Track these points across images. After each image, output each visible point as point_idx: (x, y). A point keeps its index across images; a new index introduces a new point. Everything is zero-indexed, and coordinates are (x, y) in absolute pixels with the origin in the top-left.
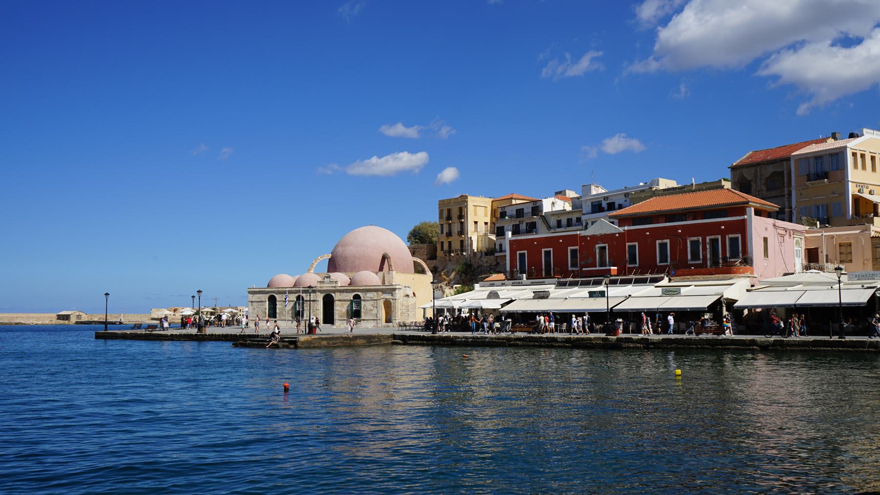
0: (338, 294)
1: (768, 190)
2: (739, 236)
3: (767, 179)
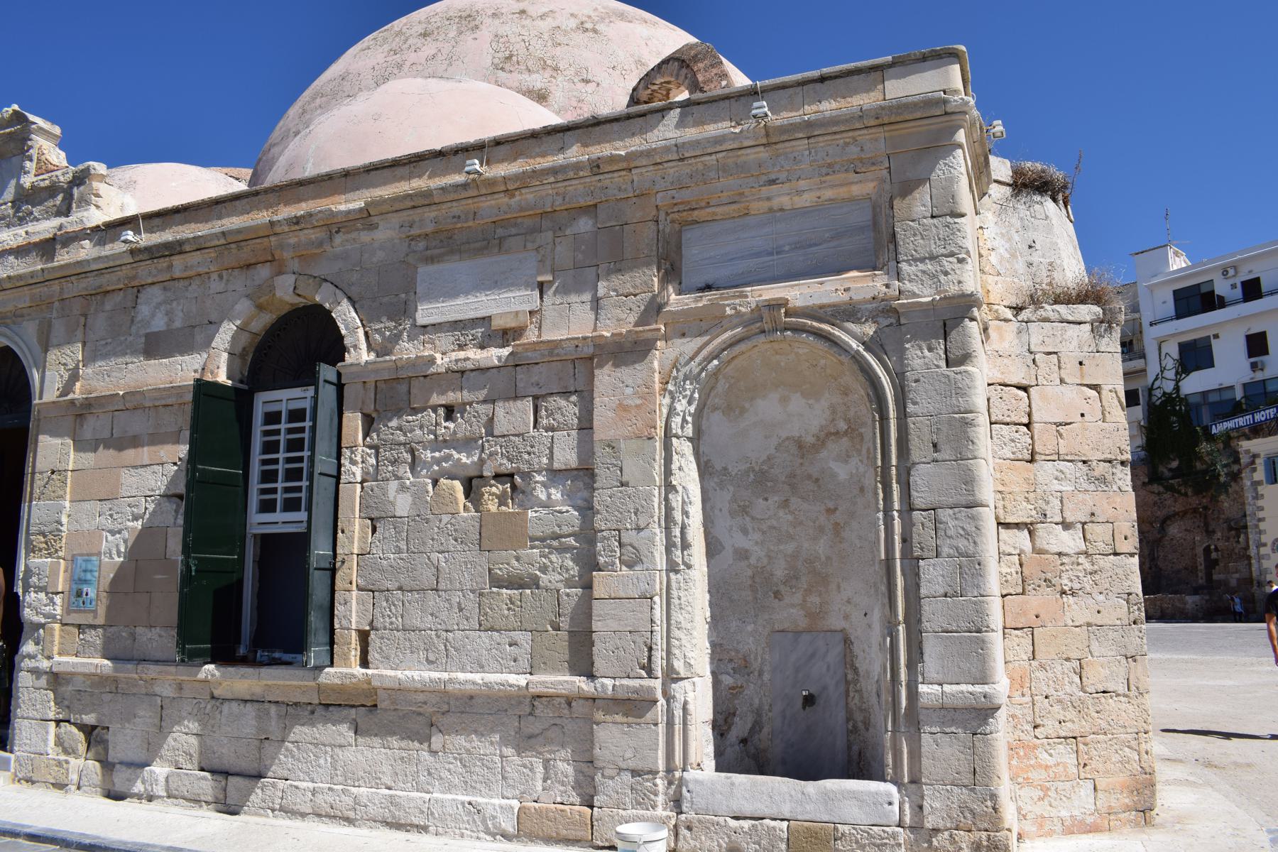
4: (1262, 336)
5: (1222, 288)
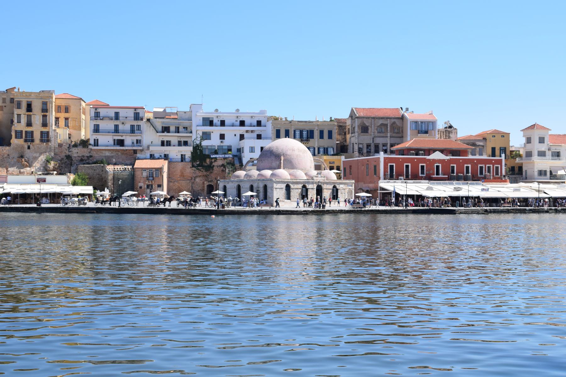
1: (378, 132)
2: (499, 166)
3: (378, 126)
5: (215, 121)
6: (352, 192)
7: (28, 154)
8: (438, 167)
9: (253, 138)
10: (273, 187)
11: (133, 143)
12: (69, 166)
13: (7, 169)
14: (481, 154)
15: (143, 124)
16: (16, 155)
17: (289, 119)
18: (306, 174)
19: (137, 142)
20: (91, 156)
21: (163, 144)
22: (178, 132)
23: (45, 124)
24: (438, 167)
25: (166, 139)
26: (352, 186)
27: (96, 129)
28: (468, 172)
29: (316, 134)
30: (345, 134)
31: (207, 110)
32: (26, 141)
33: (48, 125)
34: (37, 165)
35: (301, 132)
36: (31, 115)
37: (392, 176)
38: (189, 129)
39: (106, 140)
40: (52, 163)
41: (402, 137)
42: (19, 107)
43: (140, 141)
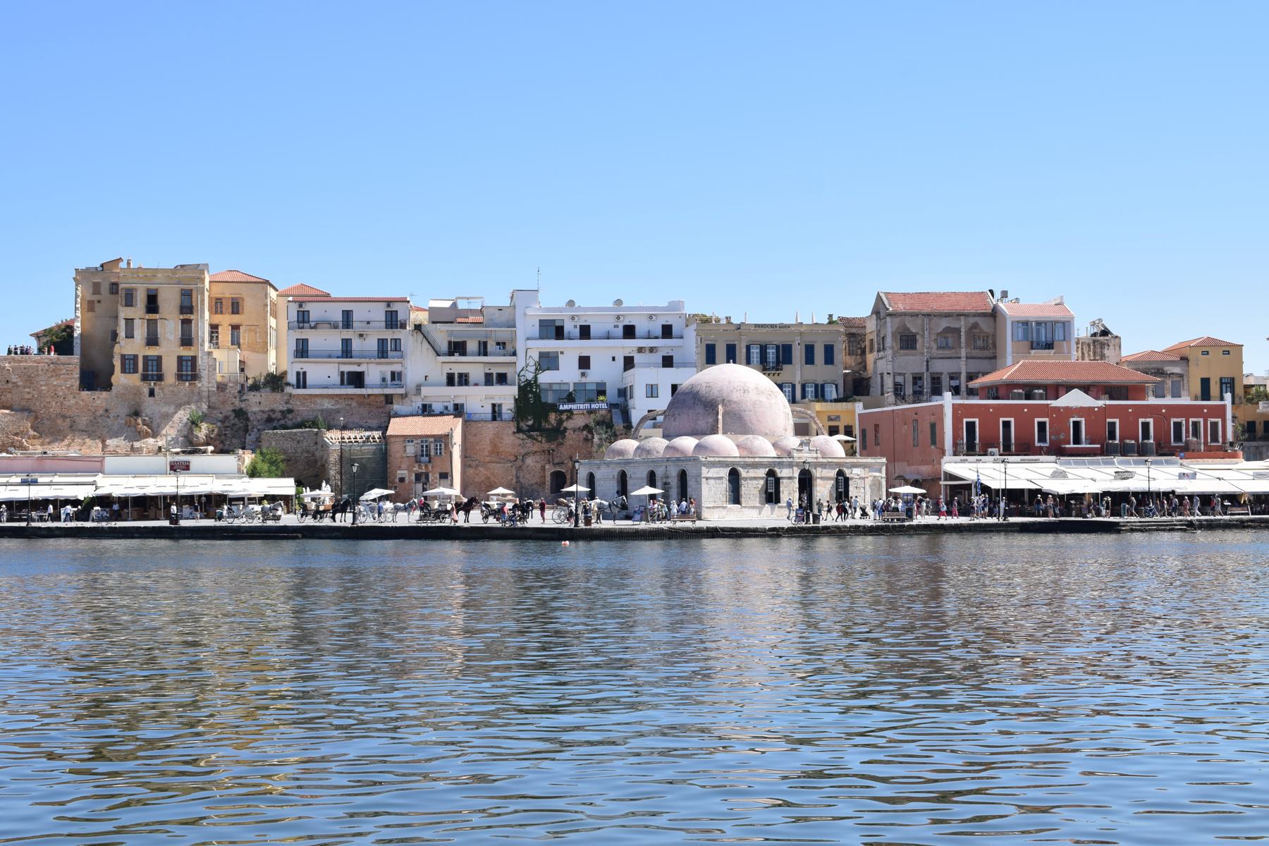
0: (819, 469)
2: (1219, 420)
4: (588, 358)
5: (569, 327)
6: (880, 484)
7: (150, 407)
8: (1077, 424)
9: (655, 365)
10: (699, 475)
11: (384, 380)
12: (241, 433)
13: (103, 442)
14: (1176, 395)
15: (405, 336)
16: (123, 411)
17: (736, 320)
18: (775, 445)
19: (393, 379)
20: (290, 411)
21: (450, 380)
22: (485, 354)
23: (187, 341)
24: (1077, 424)
25: (457, 370)
26: (880, 471)
27: (302, 350)
28: (1146, 435)
29: (798, 354)
30: (863, 352)
31: (551, 302)
32: (145, 378)
33: (195, 342)
34: (171, 431)
35: (763, 349)
36: (155, 321)
37: (971, 446)
38: (509, 348)
39: (324, 373)
40: (204, 426)
41: (995, 357)
42: (129, 301)
43: (400, 374)
